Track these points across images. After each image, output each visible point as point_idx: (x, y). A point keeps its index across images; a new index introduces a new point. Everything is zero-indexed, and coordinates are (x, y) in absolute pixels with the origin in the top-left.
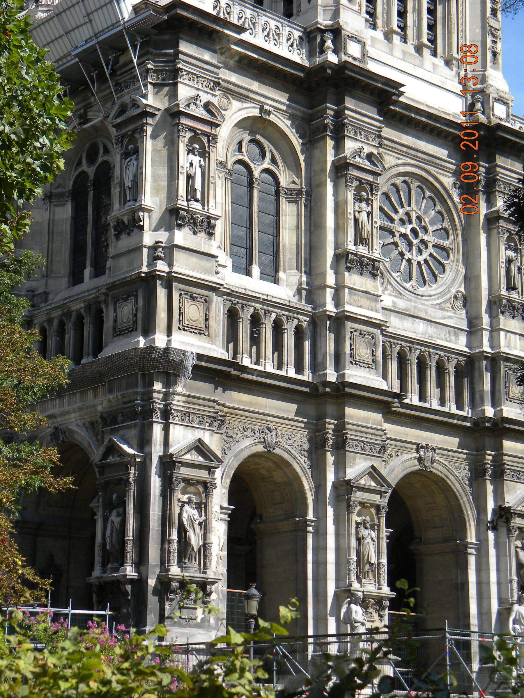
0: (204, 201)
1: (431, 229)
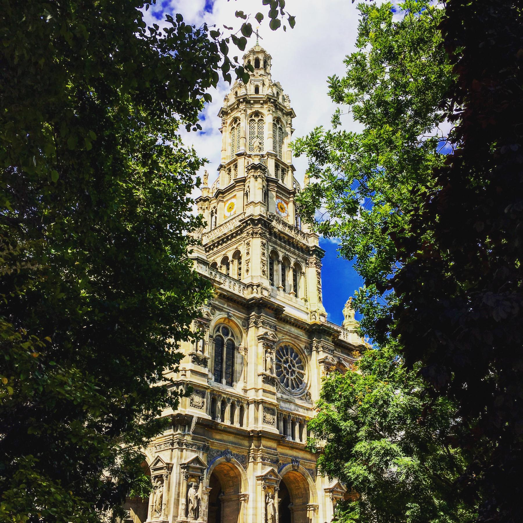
0: (203, 351)
1: (296, 365)
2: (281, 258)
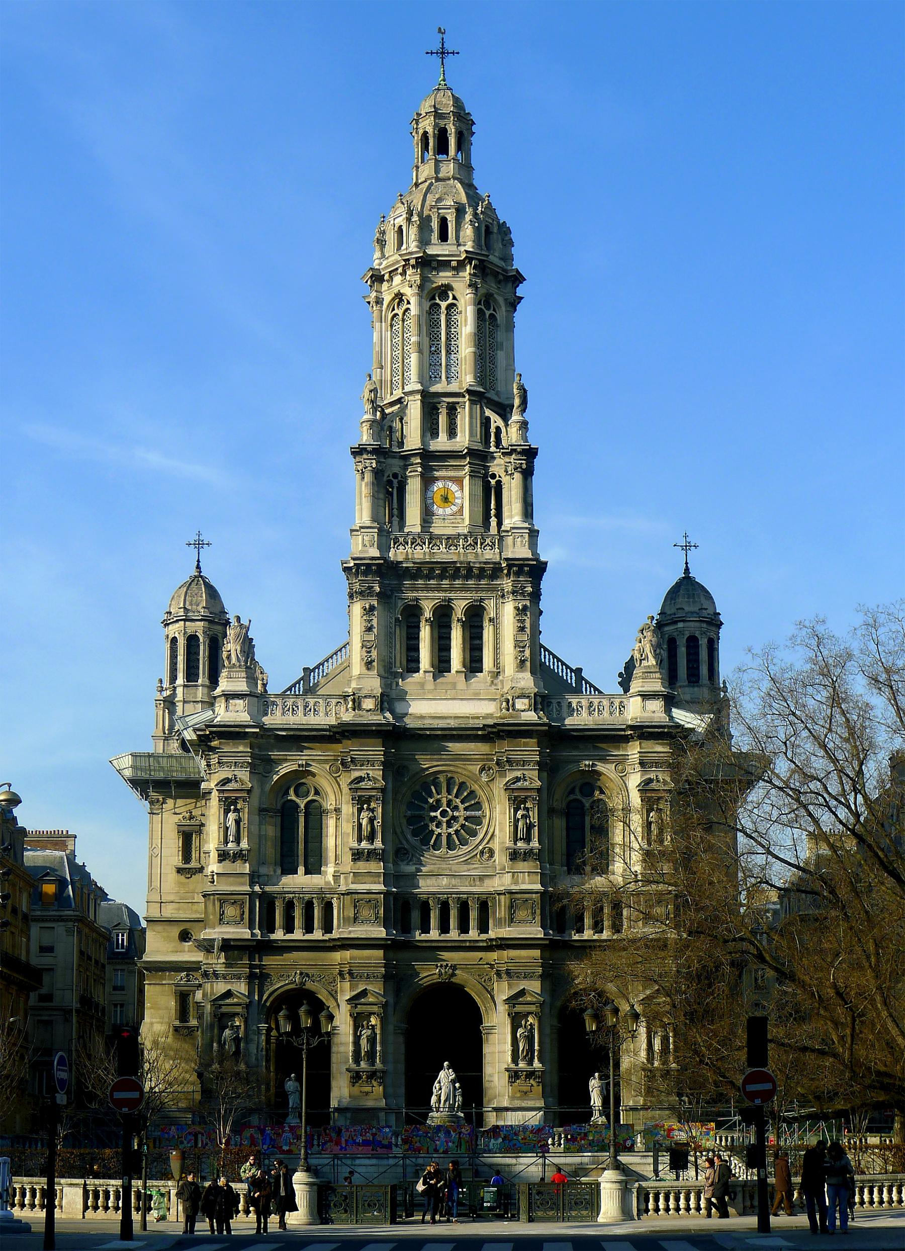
0: (238, 840)
1: (461, 807)
2: (428, 614)
